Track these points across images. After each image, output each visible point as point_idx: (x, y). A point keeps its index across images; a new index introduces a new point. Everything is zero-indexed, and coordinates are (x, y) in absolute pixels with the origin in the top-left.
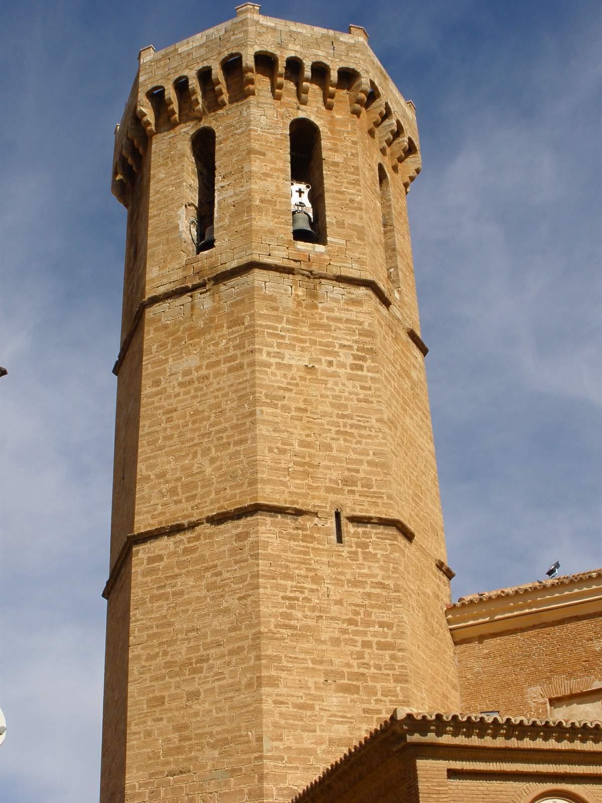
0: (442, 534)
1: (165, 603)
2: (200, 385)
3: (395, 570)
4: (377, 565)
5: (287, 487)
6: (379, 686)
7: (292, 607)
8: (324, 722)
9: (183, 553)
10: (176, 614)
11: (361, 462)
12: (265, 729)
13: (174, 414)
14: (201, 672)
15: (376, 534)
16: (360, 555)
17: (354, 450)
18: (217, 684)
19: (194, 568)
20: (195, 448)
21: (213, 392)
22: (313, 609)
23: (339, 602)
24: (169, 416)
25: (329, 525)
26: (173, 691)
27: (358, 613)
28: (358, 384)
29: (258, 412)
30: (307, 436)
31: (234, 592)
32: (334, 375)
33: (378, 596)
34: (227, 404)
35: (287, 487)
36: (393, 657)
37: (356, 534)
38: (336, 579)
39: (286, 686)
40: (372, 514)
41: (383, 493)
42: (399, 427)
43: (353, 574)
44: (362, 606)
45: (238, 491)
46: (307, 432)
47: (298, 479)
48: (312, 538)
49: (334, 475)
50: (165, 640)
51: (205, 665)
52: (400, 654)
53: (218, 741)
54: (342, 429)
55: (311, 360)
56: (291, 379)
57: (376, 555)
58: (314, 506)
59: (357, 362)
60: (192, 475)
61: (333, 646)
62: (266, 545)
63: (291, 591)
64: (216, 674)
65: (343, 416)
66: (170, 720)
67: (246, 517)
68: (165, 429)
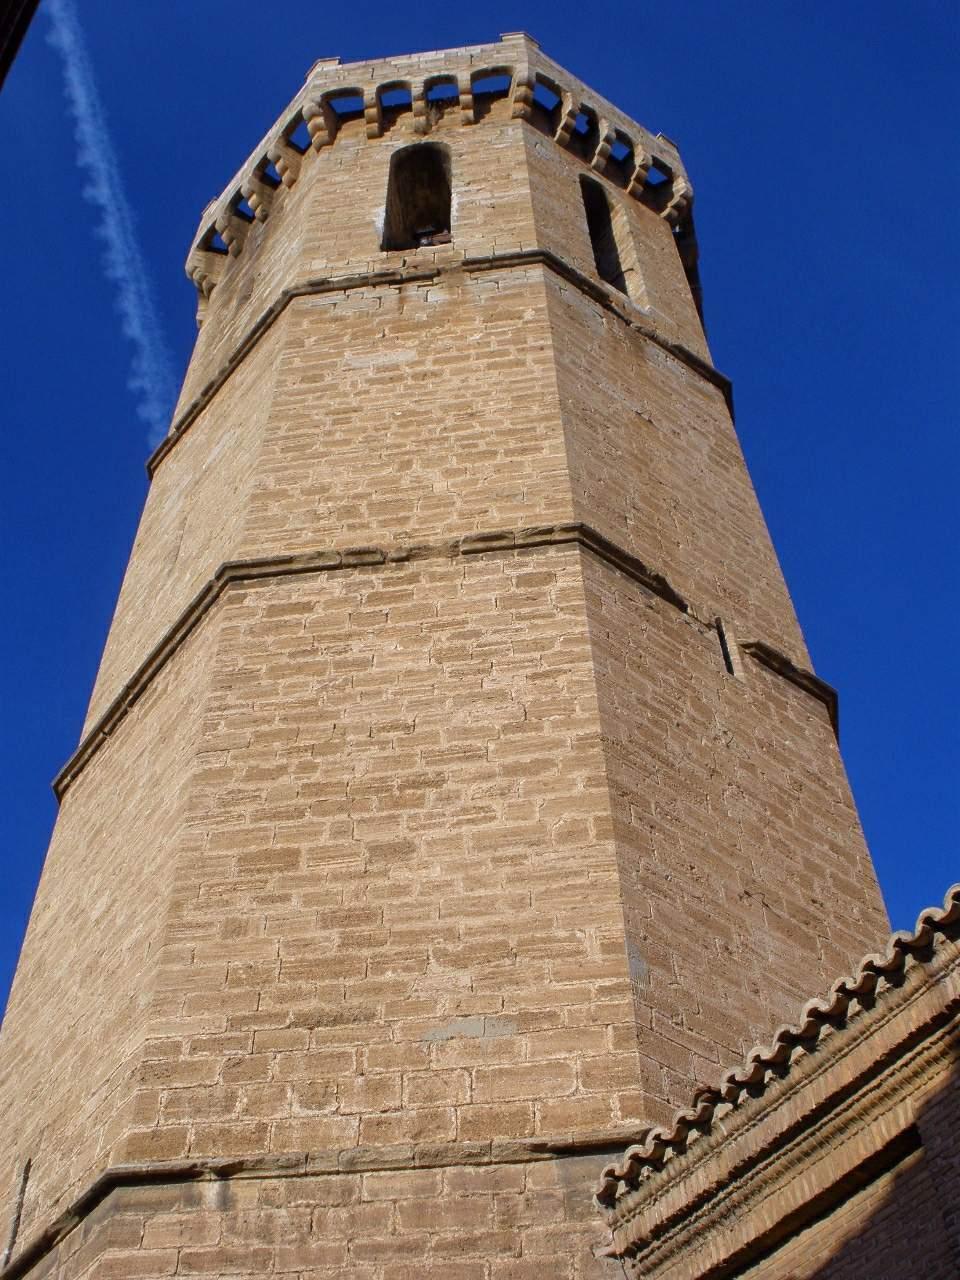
26: (324, 840)
51: (431, 793)
53: (472, 949)
64: (465, 810)
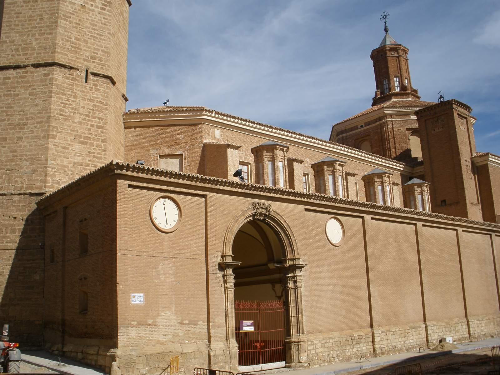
0: (125, 83)
1: (10, 98)
2: (34, 4)
3: (107, 97)
4: (100, 94)
5: (68, 56)
6: (95, 143)
7: (64, 107)
8: (72, 155)
9: (20, 78)
10: (15, 104)
11: (99, 50)
12: (49, 156)
13: (20, 15)
14: (24, 129)
15: (101, 81)
16: (94, 89)
17: (97, 45)
18: (30, 135)
19: (24, 85)
20: (29, 33)
21: (39, 9)
22: (73, 109)
23: (83, 107)
24: (17, 15)
25: (83, 75)
26: (11, 136)
27: (90, 113)
28: (102, 16)
29: (59, 22)
30: (78, 36)
31: (41, 98)
32: (93, 11)
33: (99, 106)
34: (45, 16)
35: (68, 56)
36: (102, 132)
37: (93, 80)
38: (83, 97)
39: (59, 139)
40: (101, 73)
41: (106, 64)
42: (116, 37)
43: (90, 96)
44: (92, 110)
45: (47, 55)
46: (79, 34)
47: (72, 53)
48: (75, 80)
49: (88, 54)
50: (9, 114)
51: (26, 127)
52: (105, 131)
53: (29, 158)
54: (93, 35)
55: (84, 2)
56: (74, 9)
57: (100, 89)
58: (78, 66)
59: (103, 7)
60: (26, 44)
61: (79, 125)
62: (57, 80)
63: (65, 100)
64: (30, 131)
65: (94, 29)
66: (9, 148)
67: (49, 67)
68: (15, 21)
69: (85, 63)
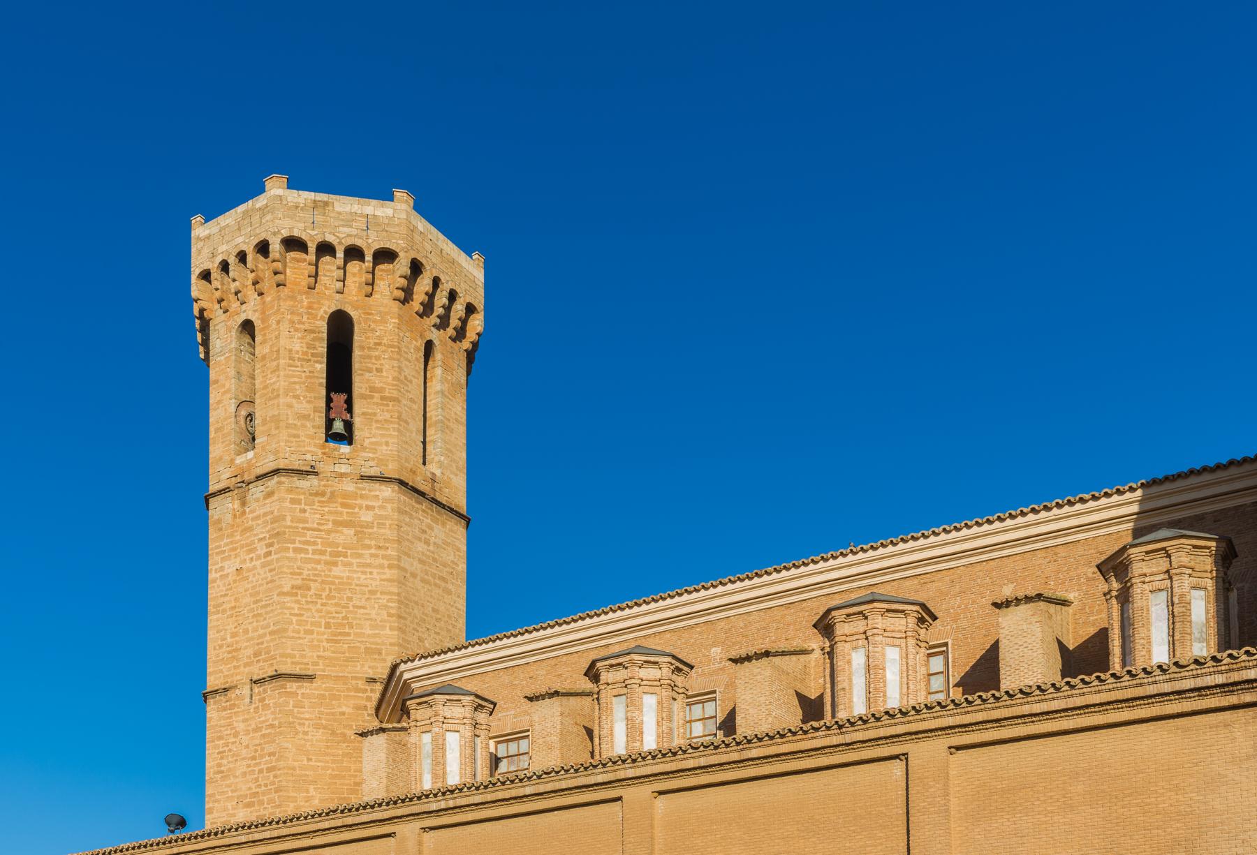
22: (233, 756)
27: (256, 751)
36: (275, 776)
69: (247, 670)
